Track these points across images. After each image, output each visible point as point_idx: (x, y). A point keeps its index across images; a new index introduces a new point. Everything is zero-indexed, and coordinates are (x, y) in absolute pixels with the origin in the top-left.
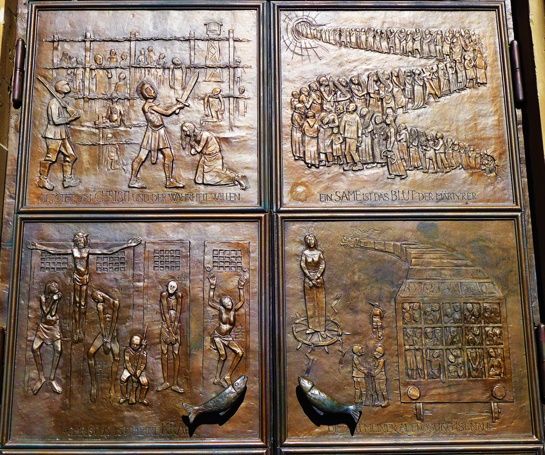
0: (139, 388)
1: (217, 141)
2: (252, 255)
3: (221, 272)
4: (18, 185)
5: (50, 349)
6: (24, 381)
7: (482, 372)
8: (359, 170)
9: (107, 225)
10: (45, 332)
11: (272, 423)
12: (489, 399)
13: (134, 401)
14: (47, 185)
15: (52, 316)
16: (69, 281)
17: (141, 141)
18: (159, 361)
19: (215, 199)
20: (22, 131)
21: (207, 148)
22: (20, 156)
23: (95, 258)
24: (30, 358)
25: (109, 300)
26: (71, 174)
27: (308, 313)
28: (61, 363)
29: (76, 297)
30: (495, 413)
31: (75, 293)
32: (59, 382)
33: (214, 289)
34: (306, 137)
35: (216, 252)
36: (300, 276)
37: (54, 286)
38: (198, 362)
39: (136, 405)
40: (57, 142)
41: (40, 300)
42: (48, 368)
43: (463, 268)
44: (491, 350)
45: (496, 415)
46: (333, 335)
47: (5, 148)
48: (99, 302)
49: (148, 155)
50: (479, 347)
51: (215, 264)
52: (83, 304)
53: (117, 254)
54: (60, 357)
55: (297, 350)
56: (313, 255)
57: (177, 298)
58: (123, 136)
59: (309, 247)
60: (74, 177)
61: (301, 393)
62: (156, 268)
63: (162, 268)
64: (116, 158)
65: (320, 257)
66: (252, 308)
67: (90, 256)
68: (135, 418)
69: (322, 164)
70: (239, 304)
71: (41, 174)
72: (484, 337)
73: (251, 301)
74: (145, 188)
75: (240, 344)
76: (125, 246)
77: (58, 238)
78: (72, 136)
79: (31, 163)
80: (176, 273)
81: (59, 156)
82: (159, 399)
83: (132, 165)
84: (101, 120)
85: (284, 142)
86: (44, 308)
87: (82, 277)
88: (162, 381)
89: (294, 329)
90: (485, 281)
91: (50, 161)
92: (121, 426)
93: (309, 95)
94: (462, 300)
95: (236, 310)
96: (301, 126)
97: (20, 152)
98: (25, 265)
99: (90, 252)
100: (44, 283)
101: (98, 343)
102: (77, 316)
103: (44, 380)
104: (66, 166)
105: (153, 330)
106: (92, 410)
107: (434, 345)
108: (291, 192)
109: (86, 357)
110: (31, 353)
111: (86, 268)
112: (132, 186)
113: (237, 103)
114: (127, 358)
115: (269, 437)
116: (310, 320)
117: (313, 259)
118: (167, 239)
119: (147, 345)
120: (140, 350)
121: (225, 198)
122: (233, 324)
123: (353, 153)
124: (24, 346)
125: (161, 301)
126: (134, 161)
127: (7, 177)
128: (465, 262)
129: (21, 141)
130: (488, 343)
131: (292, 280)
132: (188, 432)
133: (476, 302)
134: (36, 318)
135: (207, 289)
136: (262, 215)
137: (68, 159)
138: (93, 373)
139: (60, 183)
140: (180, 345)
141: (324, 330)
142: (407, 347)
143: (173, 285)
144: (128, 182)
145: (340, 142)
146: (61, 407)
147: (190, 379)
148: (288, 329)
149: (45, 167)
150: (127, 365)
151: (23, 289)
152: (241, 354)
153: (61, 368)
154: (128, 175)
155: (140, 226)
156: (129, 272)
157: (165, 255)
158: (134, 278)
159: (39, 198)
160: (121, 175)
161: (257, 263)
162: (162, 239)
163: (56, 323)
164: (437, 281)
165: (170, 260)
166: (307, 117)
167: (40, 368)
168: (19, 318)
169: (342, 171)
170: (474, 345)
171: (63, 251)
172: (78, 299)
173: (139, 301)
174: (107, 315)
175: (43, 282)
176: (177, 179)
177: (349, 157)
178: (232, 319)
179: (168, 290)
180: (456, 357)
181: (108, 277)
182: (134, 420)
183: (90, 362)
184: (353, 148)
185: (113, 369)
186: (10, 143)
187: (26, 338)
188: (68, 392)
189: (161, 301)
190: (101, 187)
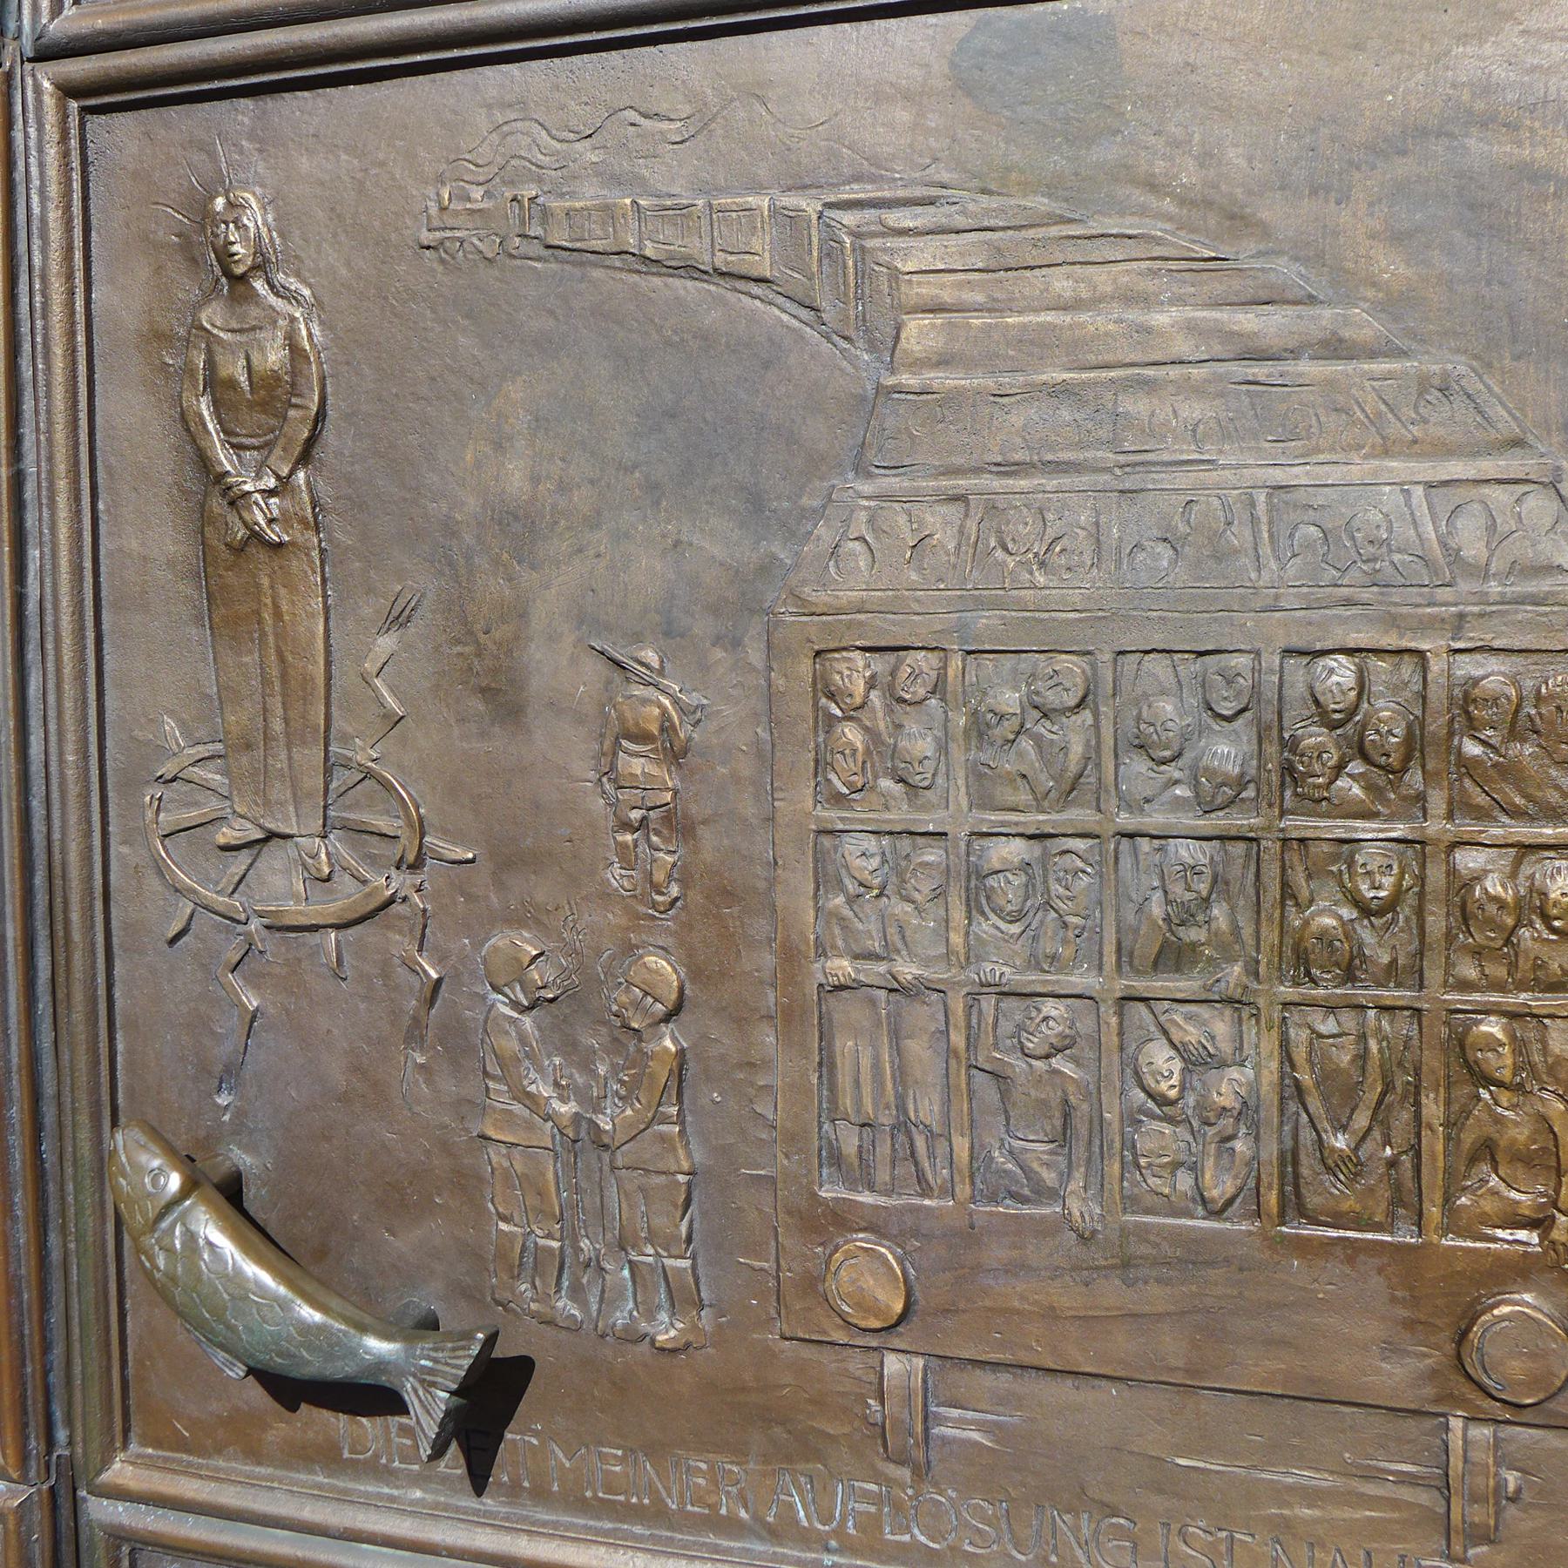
7: (1397, 1187)
12: (1429, 1391)
30: (1475, 1498)
43: (1307, 368)
44: (1493, 1027)
45: (1480, 1514)
50: (1390, 995)
72: (1436, 922)
90: (1489, 466)
107: (1034, 963)
128: (1326, 316)
130: (1470, 971)
133: (1391, 641)
142: (843, 967)
164: (1085, 480)
170: (1349, 977)
180: (1197, 1062)
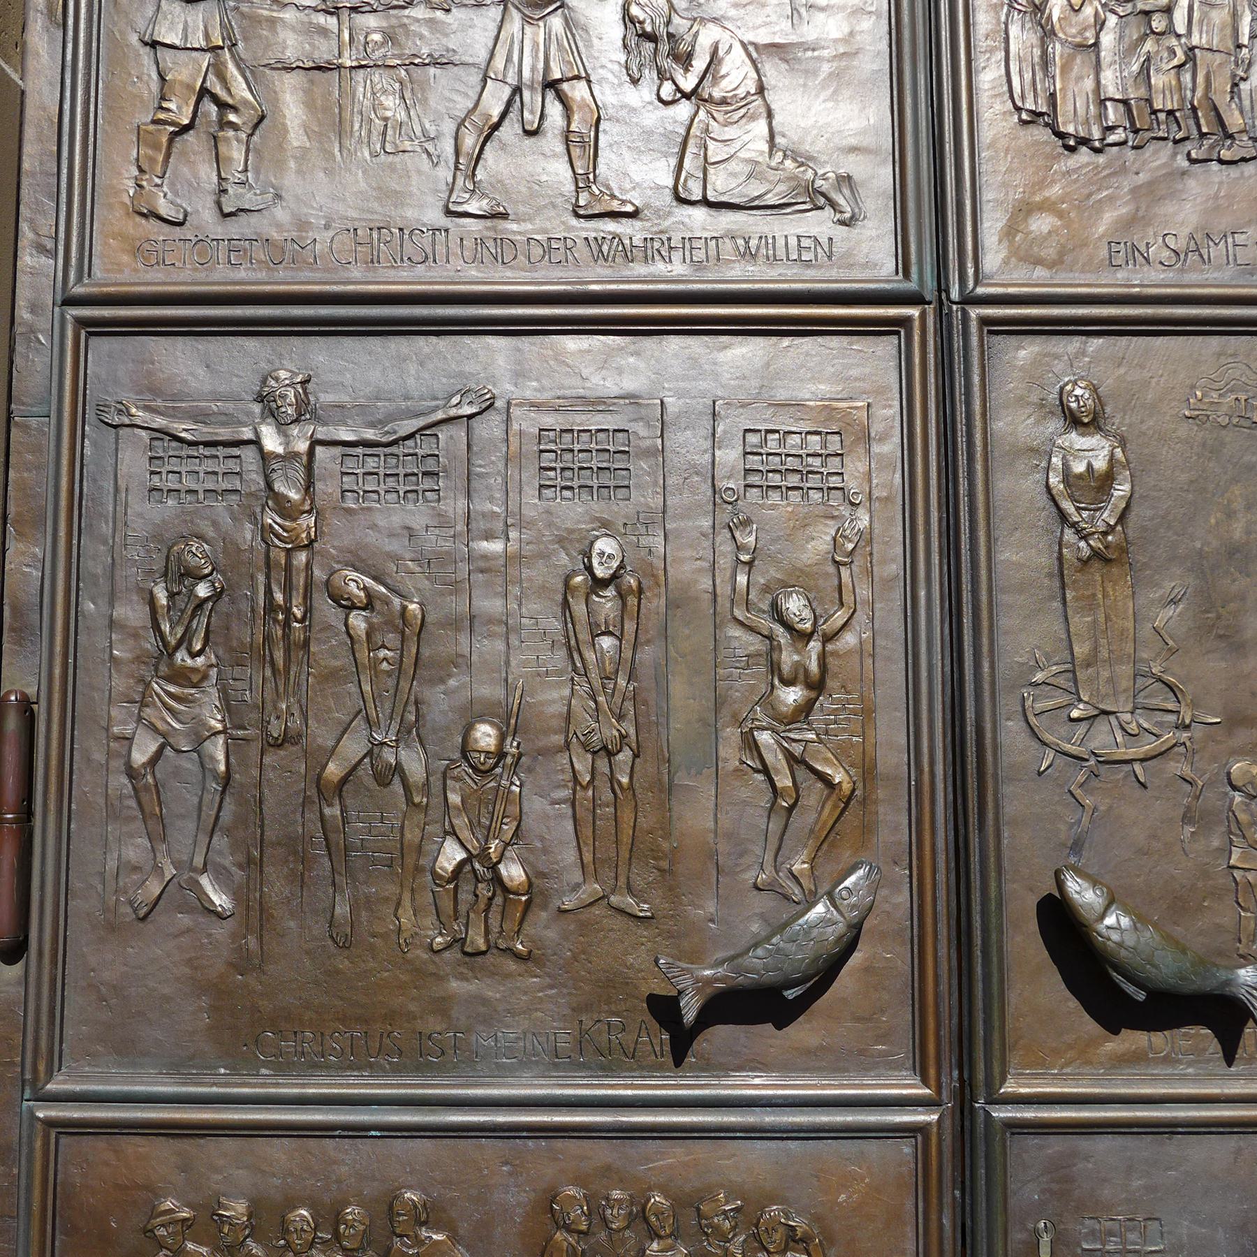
0: (499, 900)
1: (749, 56)
2: (876, 449)
3: (773, 507)
4: (63, 207)
5: (189, 764)
6: (102, 875)
8: (1244, 160)
9: (374, 343)
10: (170, 710)
11: (955, 1020)
13: (481, 944)
14: (164, 209)
15: (194, 655)
16: (247, 534)
17: (483, 55)
18: (566, 809)
19: (749, 255)
20: (71, 21)
21: (716, 80)
22: (67, 106)
23: (334, 458)
24: (121, 797)
25: (387, 602)
26: (246, 170)
27: (1076, 649)
28: (227, 816)
29: (275, 588)
31: (268, 577)
32: (222, 878)
33: (750, 564)
34: (1058, 46)
35: (753, 439)
37: (197, 554)
38: (697, 815)
39: (489, 959)
40: (195, 60)
41: (152, 601)
42: (184, 833)
46: (1160, 724)
47: (15, 77)
48: (353, 607)
49: (509, 104)
51: (754, 479)
52: (298, 612)
53: (410, 443)
54: (223, 792)
55: (1040, 774)
56: (1092, 451)
57: (621, 596)
58: (421, 37)
59: (1074, 421)
60: (257, 180)
61: (1059, 919)
62: (548, 493)
63: (567, 493)
64: (401, 115)
65: (1112, 455)
66: (874, 631)
67: (319, 450)
68: (485, 1001)
69: (1112, 138)
70: (840, 617)
71: (141, 170)
73: (877, 606)
74: (504, 216)
75: (841, 754)
76: (440, 415)
77: (207, 388)
78: (245, 39)
79: (105, 131)
80: (619, 509)
81: (201, 108)
82: (566, 938)
83: (456, 139)
85: (980, 61)
86: (166, 627)
87: (295, 520)
88: (577, 876)
89: (1028, 703)
91: (172, 124)
92: (438, 1029)
95: (828, 638)
97: (68, 94)
98: (95, 480)
99: (319, 436)
100: (161, 541)
101: (353, 747)
102: (279, 656)
103: (170, 871)
104: (227, 140)
105: (542, 704)
106: (338, 972)
108: (1010, 232)
109: (312, 792)
110: (124, 780)
111: (307, 489)
112: (460, 209)
114: (455, 798)
115: (946, 1065)
116: (1080, 675)
117: (1090, 465)
118: (582, 392)
119: (520, 755)
120: (498, 770)
121: (781, 253)
122: (817, 686)
123: (1222, 100)
124: (99, 756)
125: (566, 604)
126: (461, 124)
127: (26, 182)
129: (69, 57)
131: (1018, 534)
132: (667, 1048)
134: (138, 659)
135: (725, 562)
136: (914, 312)
137: (232, 117)
138: (340, 851)
139: (210, 201)
140: (636, 756)
141: (1130, 707)
143: (608, 551)
144: (445, 195)
145: (1176, 62)
146: (230, 964)
147: (671, 872)
148: (1008, 703)
149: (156, 147)
150: (456, 822)
151: (90, 563)
152: (847, 787)
153: (228, 832)
154: (444, 173)
155: (487, 347)
156: (455, 506)
157: (577, 447)
158: (473, 525)
159: (136, 251)
160: (419, 172)
161: (898, 475)
162: (568, 393)
163: (205, 677)
165: (594, 464)
167: (158, 828)
168: (80, 661)
169: (1182, 162)
171: (224, 433)
172: (279, 597)
173: (491, 605)
174: (383, 653)
175: (157, 537)
176: (613, 185)
177: (1205, 116)
178: (814, 666)
179: (589, 568)
181: (382, 523)
182: (482, 1009)
183: (327, 811)
184: (1222, 84)
185: (408, 835)
186: (31, 63)
187: (107, 730)
188: (254, 911)
189: (566, 604)
190: (353, 214)
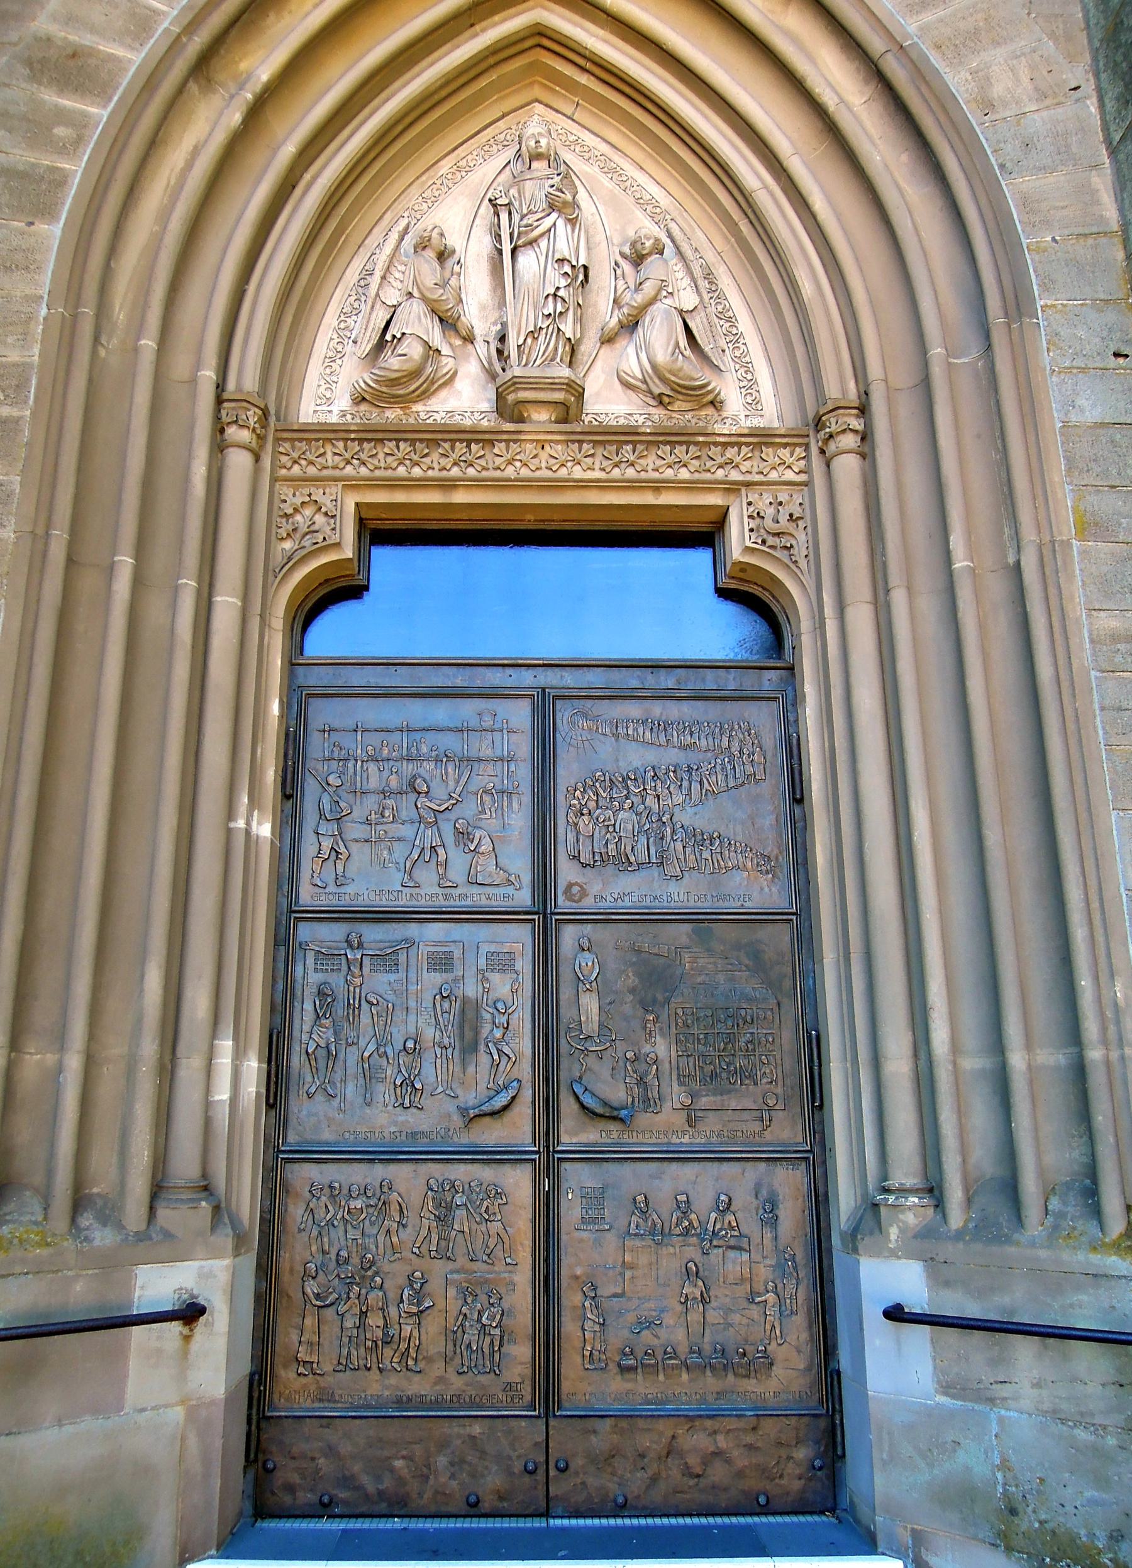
36: (574, 979)
84: (373, 816)
93: (585, 791)
94: (736, 1005)
96: (576, 824)
113: (511, 799)
136: (536, 917)
166: (582, 814)
180: (728, 1064)
